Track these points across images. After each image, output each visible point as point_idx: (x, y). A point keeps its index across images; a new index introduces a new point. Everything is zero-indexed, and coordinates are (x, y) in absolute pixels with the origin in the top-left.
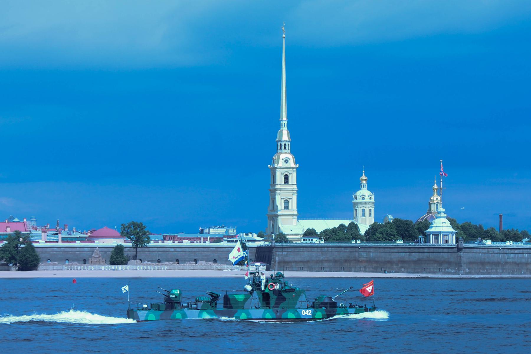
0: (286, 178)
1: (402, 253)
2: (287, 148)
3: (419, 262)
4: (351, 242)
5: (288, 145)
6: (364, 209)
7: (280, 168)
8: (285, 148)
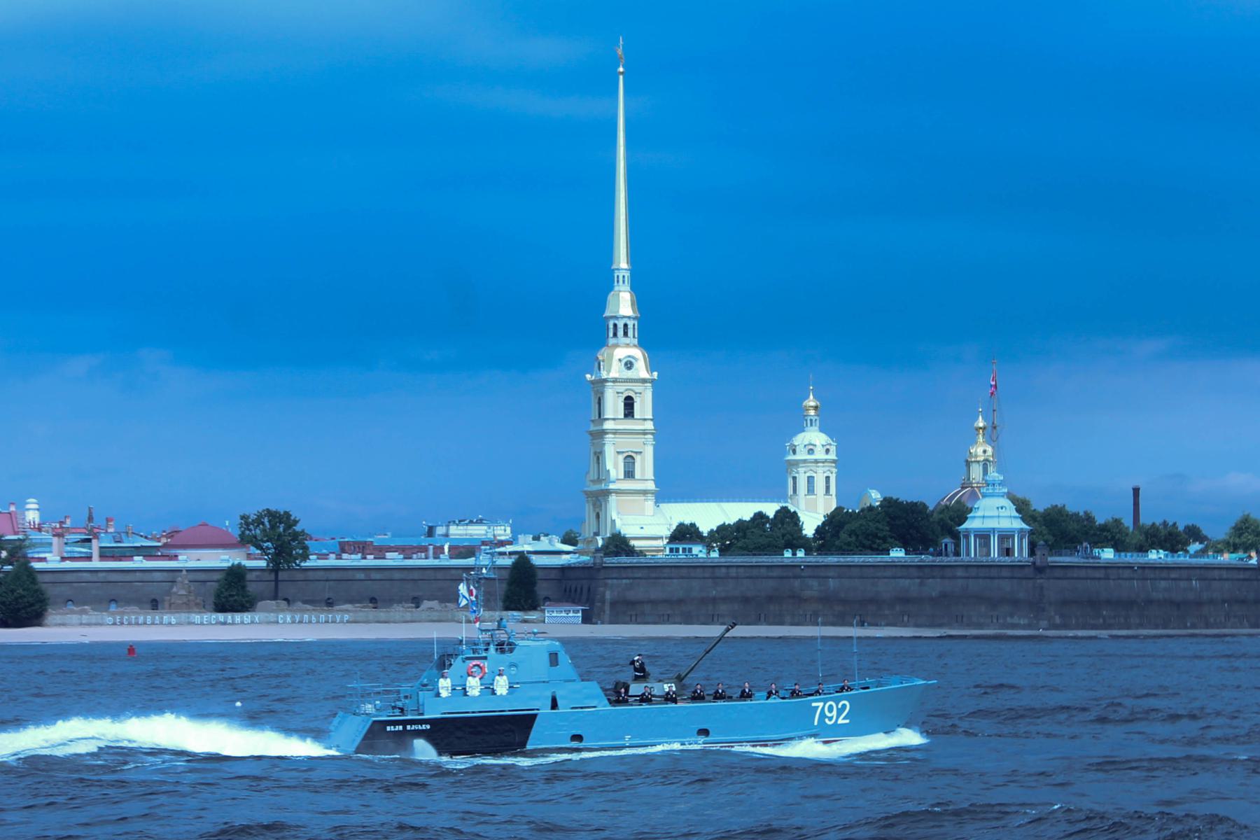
0: (629, 404)
1: (903, 580)
2: (630, 333)
3: (944, 600)
4: (783, 555)
5: (632, 326)
6: (813, 477)
7: (615, 381)
8: (626, 334)
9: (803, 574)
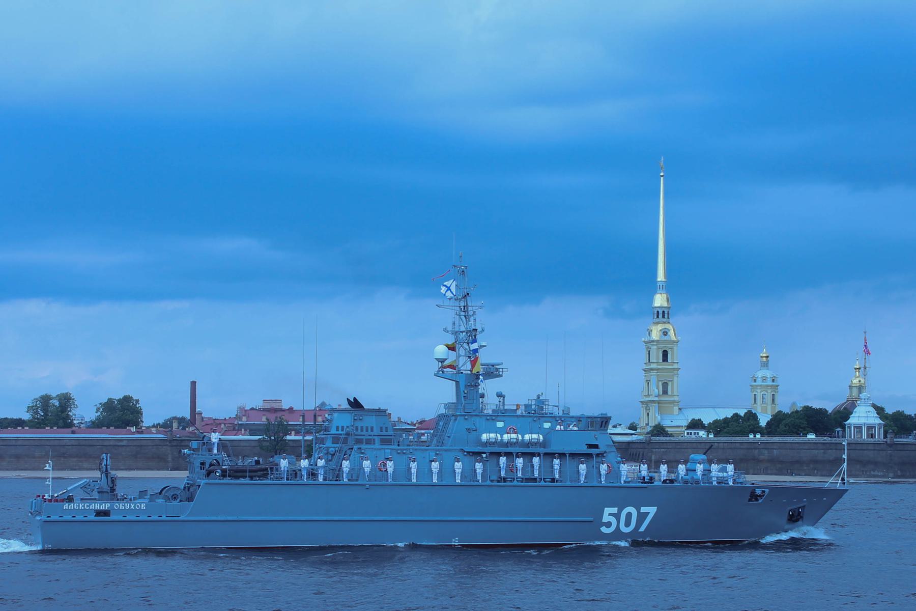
6: (765, 394)
8: (663, 317)
9: (760, 447)
